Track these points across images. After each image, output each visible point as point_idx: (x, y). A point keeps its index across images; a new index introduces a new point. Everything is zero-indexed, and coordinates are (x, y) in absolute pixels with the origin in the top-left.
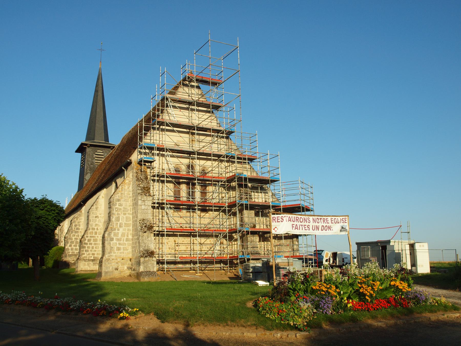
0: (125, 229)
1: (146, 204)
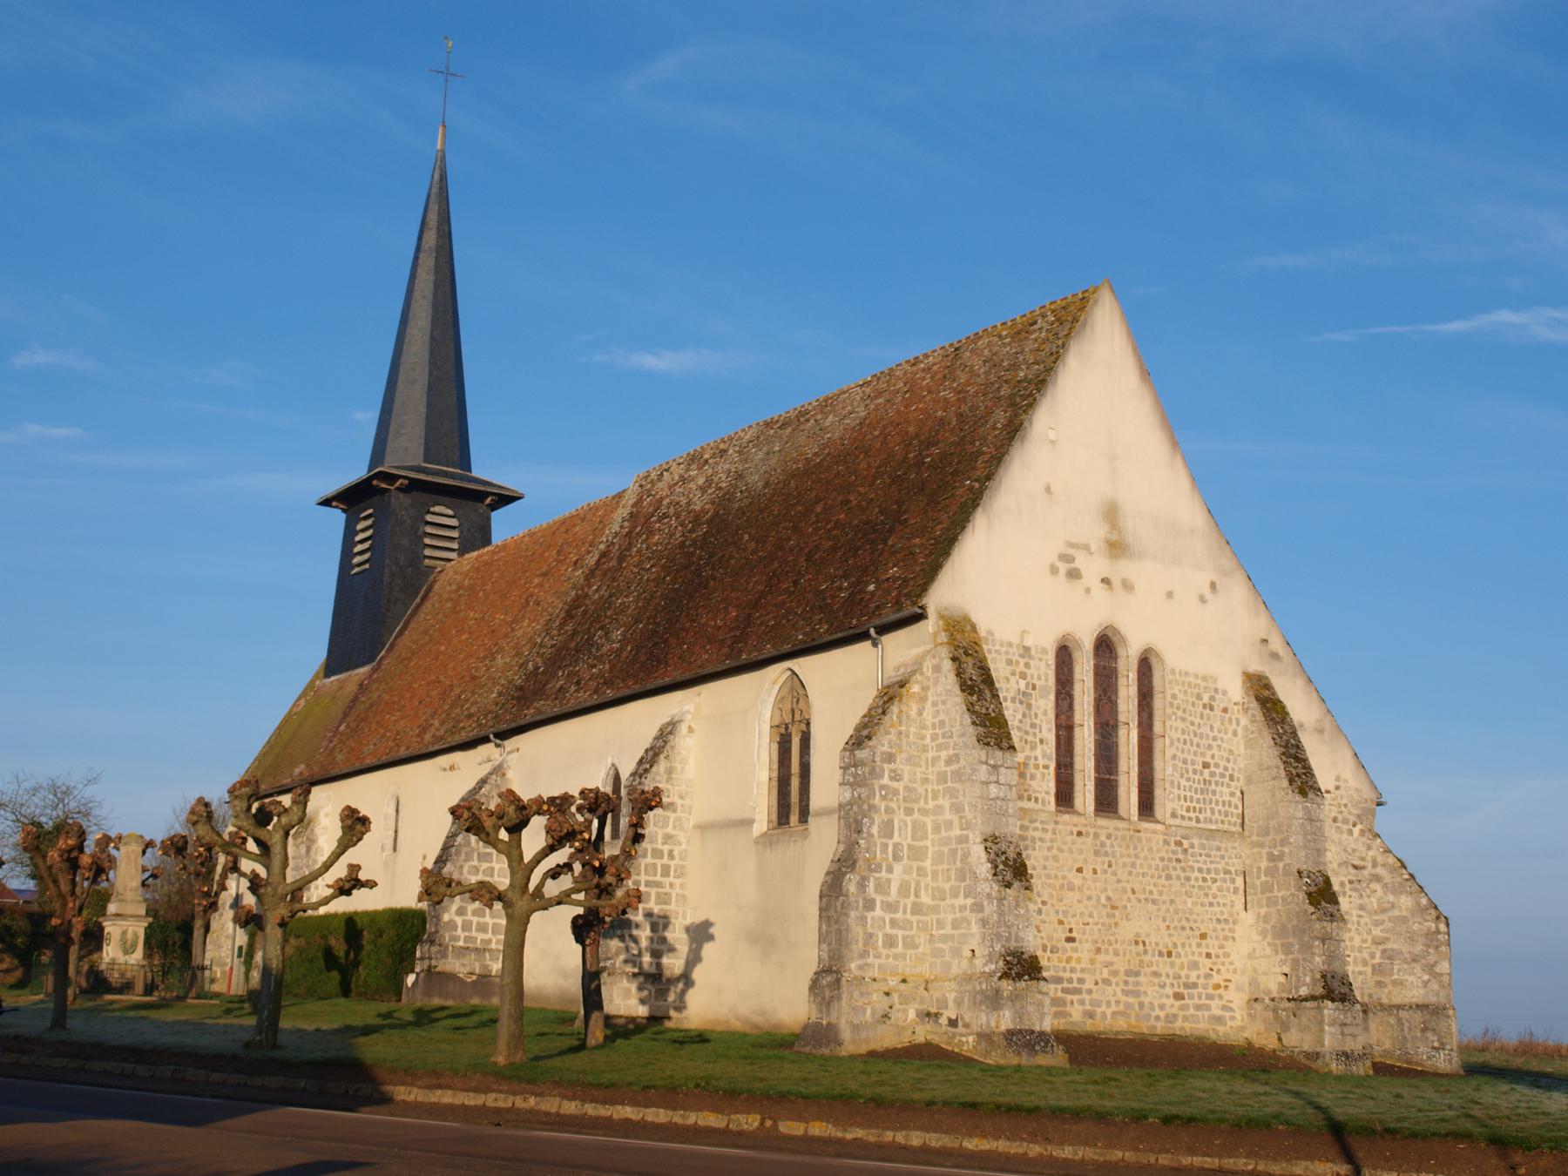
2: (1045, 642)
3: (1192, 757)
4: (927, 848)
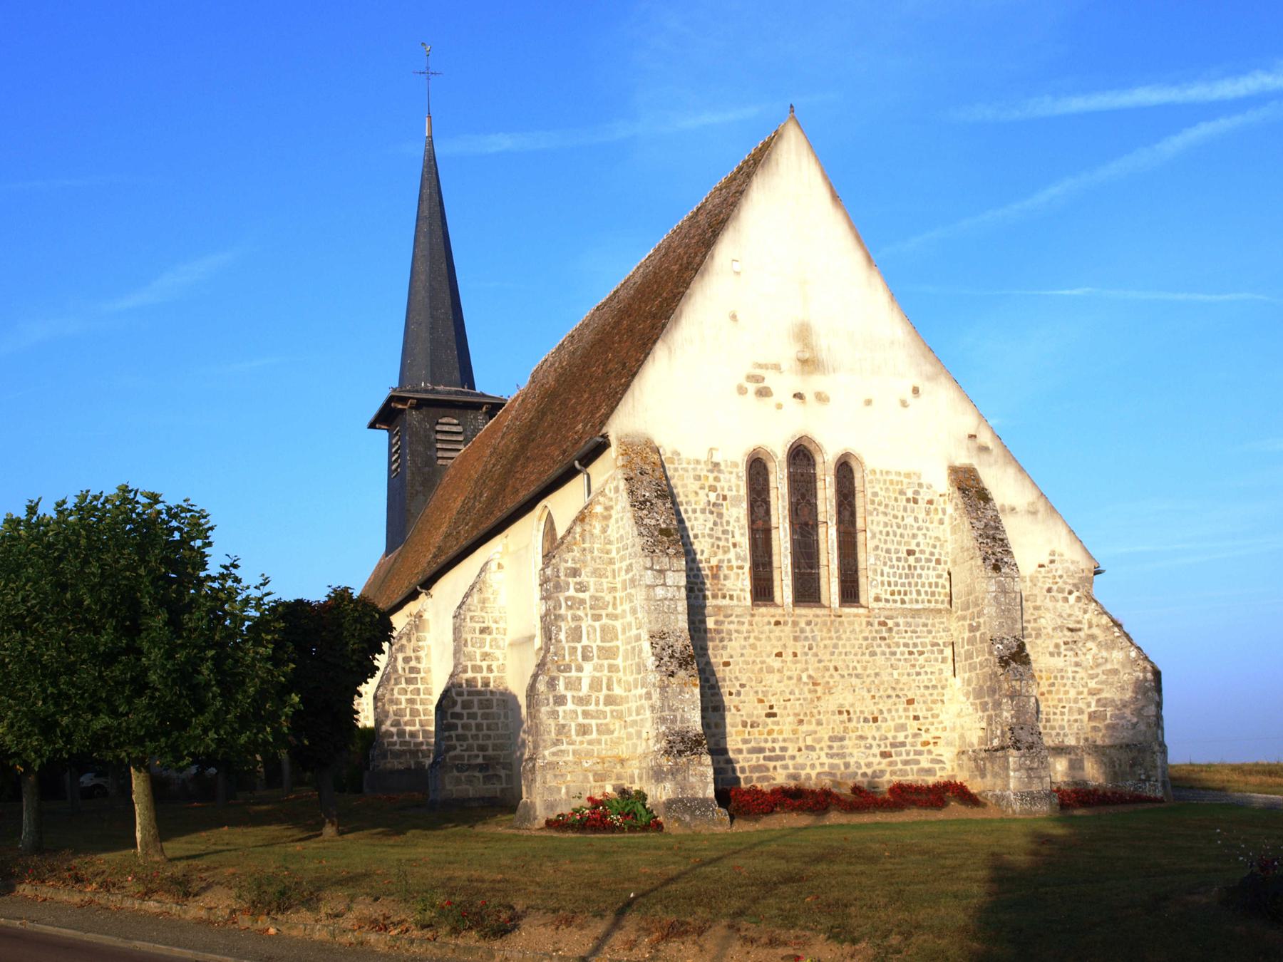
0: (602, 666)
1: (669, 582)
2: (735, 458)
3: (896, 546)
4: (618, 648)
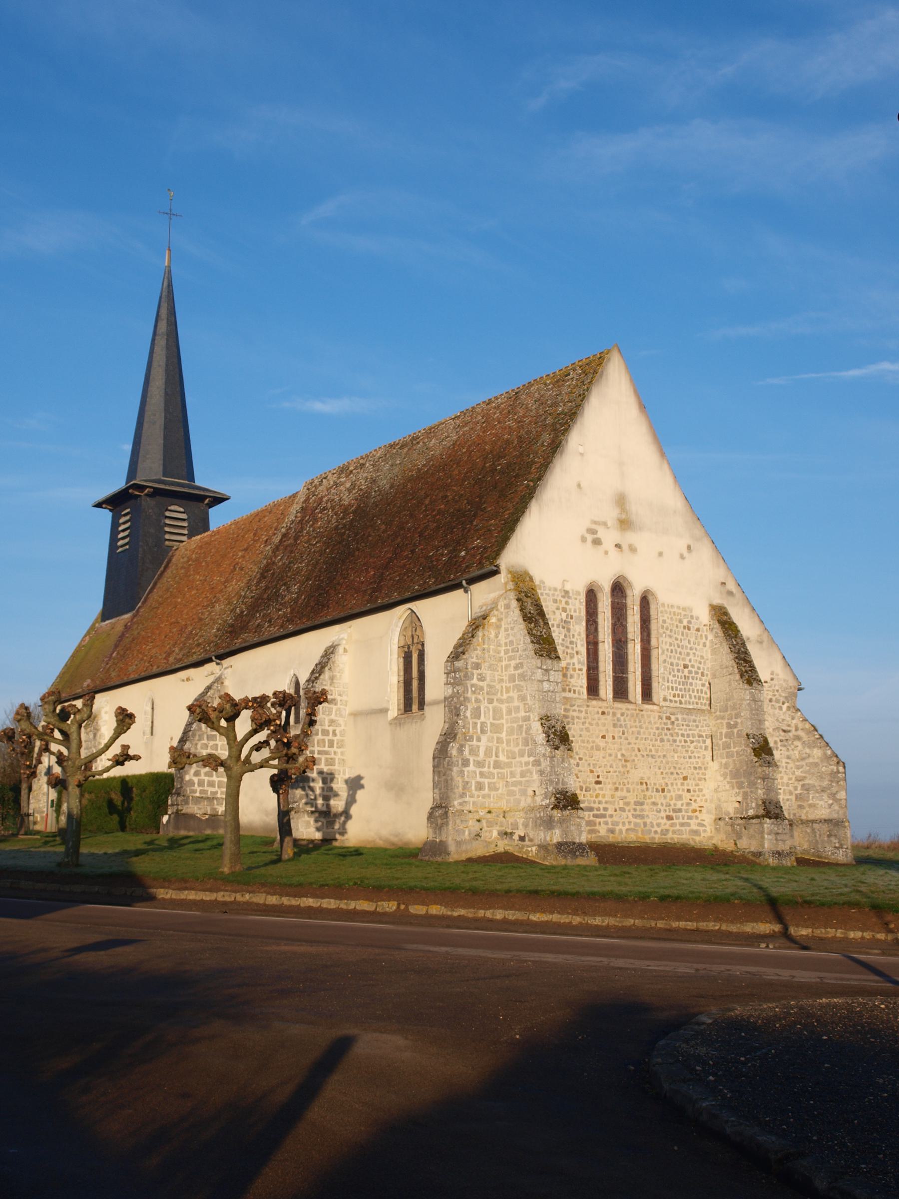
2: (579, 587)
